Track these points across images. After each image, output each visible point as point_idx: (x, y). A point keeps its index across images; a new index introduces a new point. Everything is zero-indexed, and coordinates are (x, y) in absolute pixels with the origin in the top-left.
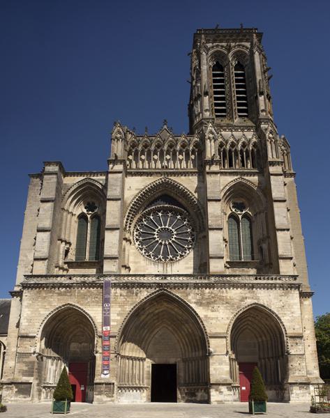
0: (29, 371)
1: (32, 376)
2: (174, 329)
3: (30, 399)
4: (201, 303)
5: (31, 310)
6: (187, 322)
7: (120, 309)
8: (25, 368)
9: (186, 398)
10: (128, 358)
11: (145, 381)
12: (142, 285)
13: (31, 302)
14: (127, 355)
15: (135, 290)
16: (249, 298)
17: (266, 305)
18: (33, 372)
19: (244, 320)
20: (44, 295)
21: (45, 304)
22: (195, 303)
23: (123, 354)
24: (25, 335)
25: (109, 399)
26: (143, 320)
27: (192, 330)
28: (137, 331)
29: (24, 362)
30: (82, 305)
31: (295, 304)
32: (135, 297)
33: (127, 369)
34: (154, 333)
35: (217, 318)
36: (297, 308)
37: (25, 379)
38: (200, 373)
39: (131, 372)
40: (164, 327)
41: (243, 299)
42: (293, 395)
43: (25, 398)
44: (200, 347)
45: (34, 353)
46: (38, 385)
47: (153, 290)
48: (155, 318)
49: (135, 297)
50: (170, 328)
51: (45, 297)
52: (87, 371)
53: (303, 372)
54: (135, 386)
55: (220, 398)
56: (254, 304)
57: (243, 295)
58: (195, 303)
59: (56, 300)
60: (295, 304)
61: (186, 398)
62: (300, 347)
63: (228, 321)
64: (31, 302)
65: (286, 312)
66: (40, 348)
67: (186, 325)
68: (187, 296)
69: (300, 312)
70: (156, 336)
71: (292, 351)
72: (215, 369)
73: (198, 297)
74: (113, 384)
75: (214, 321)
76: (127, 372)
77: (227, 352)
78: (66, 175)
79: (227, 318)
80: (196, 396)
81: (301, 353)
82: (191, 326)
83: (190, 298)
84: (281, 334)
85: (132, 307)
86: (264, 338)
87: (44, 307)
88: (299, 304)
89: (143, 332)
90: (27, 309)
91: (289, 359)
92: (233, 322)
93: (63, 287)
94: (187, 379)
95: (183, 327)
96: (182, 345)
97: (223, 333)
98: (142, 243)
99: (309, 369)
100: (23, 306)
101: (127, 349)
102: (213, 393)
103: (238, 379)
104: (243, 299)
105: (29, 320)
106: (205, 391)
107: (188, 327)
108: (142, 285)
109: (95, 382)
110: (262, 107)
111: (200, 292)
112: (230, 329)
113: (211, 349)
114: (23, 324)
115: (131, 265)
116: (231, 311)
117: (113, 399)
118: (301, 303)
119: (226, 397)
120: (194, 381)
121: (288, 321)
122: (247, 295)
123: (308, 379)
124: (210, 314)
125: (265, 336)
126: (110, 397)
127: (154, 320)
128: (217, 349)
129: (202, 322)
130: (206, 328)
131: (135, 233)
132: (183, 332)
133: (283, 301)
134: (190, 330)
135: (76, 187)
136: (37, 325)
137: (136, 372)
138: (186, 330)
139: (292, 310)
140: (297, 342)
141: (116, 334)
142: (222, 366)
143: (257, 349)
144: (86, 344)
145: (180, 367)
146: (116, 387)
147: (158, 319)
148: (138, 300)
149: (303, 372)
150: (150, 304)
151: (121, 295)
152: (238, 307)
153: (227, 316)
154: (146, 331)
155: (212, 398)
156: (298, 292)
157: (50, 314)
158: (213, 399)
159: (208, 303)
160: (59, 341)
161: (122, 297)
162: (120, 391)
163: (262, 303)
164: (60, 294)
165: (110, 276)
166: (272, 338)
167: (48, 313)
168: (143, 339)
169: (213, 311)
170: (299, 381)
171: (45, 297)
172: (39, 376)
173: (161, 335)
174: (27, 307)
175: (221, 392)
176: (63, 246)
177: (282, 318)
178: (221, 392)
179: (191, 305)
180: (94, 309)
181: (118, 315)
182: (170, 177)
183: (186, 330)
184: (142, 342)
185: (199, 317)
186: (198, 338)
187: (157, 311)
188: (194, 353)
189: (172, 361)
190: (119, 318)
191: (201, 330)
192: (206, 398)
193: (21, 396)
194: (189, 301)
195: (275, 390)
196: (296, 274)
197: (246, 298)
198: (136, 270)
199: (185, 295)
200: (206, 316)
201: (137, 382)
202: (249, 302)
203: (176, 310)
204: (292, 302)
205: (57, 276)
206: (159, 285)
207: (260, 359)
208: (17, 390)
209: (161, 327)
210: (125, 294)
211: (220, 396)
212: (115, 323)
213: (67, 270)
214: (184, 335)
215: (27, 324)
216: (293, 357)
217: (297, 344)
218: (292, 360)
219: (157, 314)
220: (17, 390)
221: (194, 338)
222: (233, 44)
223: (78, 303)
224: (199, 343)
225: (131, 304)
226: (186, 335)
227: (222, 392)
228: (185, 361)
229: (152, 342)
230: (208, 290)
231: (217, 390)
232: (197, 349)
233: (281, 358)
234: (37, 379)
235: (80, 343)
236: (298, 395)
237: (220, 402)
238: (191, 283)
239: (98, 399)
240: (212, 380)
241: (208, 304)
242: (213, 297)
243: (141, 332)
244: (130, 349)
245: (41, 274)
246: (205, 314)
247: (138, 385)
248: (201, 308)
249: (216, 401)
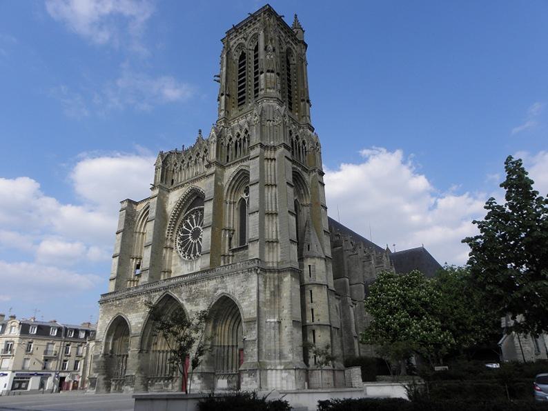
3: (95, 391)
8: (96, 367)
31: (253, 288)
47: (161, 293)
60: (253, 288)
62: (254, 332)
78: (137, 204)
98: (182, 246)
110: (262, 87)
115: (173, 269)
122: (219, 286)
131: (178, 238)
135: (142, 211)
139: (251, 294)
164: (116, 306)
169: (196, 306)
176: (134, 263)
182: (195, 184)
198: (175, 272)
202: (219, 292)
213: (138, 281)
222: (248, 31)
230: (193, 287)
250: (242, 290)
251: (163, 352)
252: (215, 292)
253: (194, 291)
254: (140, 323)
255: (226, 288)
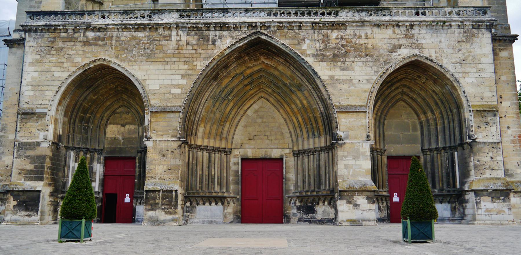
0: (37, 172)
1: (41, 179)
2: (278, 101)
3: (37, 218)
4: (324, 56)
5: (40, 69)
6: (299, 87)
7: (186, 67)
9: (299, 215)
10: (202, 149)
11: (232, 187)
12: (223, 26)
13: (38, 57)
14: (199, 143)
15: (211, 34)
16: (405, 46)
17: (434, 58)
18: (42, 173)
19: (398, 85)
20: (61, 44)
21: (63, 60)
22: (313, 55)
23: (193, 142)
24: (29, 111)
25: (169, 217)
26: (226, 87)
27: (309, 102)
28: (217, 105)
29: (28, 157)
30: (122, 60)
32: (210, 46)
33: (199, 167)
34: (245, 108)
35: (351, 80)
36: (488, 62)
37: (29, 185)
38: (323, 173)
39: (206, 173)
40: (263, 91)
41: (394, 48)
42: (480, 212)
43: (29, 216)
44: (321, 129)
45: (46, 140)
46: (52, 194)
48: (246, 82)
49: (210, 46)
50: (271, 99)
51: (61, 49)
52: (135, 171)
53: (499, 172)
54: (214, 194)
55: (355, 215)
56: (414, 56)
57: (395, 42)
58: (313, 55)
59: (81, 52)
60: (485, 56)
61: (299, 215)
62: (493, 129)
63: (368, 87)
64: (38, 57)
65: (468, 70)
66: (55, 133)
67: (299, 94)
68: (299, 43)
69: (493, 70)
70: (249, 112)
71: (480, 137)
72: (346, 166)
73: (319, 46)
74: (176, 191)
75: (344, 86)
76: (199, 172)
77: (368, 136)
79: (368, 81)
80: (314, 212)
81: (496, 139)
82: (307, 95)
83: (304, 47)
84: (459, 107)
85: (207, 63)
86: (429, 114)
87: (60, 65)
88: (491, 56)
89: (227, 105)
90: (32, 69)
91: (475, 149)
92: (377, 87)
93: (94, 30)
94: (300, 183)
95: (295, 98)
96: (291, 127)
97: (361, 106)
99: (508, 167)
100: (26, 64)
101: (200, 133)
102: (342, 205)
103: (386, 184)
104: (394, 48)
105: (36, 87)
106: (329, 204)
107: (302, 98)
108: (223, 26)
109: (145, 188)
111: (321, 37)
112: (373, 98)
113: (340, 133)
114: (26, 93)
116: (375, 68)
117: (176, 216)
118: (495, 54)
119: (365, 212)
120: (312, 188)
121: (473, 85)
122: (403, 42)
123: (508, 183)
124: (338, 74)
125: (432, 111)
126: (171, 213)
127: (246, 86)
128: (351, 133)
129: (324, 86)
130: (332, 97)
132: (293, 106)
133: (464, 50)
134: (305, 102)
136: (49, 94)
137: (216, 172)
138: (298, 102)
139: (480, 66)
140: (489, 119)
141: (181, 109)
142: (358, 162)
143: (419, 133)
144: (132, 127)
145: (290, 162)
146: (180, 198)
147: (251, 83)
148: (216, 52)
149: (499, 172)
150: (237, 58)
151: (188, 44)
152: (386, 63)
153: (367, 78)
154: (231, 104)
155: (340, 214)
156: (489, 36)
157: (70, 75)
158: (342, 217)
159: (335, 55)
160: (88, 122)
161: (190, 47)
162: (188, 204)
163: (427, 55)
164: (86, 43)
165: (170, 11)
166: (445, 114)
167: (66, 74)
168: (227, 117)
169: (343, 69)
170: (492, 187)
171: (61, 49)
172: (53, 180)
173: (256, 111)
174: (32, 64)
175: (356, 206)
177: (461, 81)
178: (356, 206)
179: (308, 59)
180: (145, 67)
181: (183, 76)
183: (298, 102)
184: (225, 121)
185: (319, 78)
186: (318, 115)
187: (248, 72)
188: (311, 141)
189: (275, 153)
190: (184, 82)
191: (323, 100)
192: (332, 216)
193: (23, 213)
194: (304, 52)
195: (449, 202)
196: (486, 5)
197: (400, 46)
199: (296, 42)
200: (332, 78)
201: (217, 188)
203: (280, 68)
204: (478, 52)
205: (82, 14)
206: (251, 26)
207: (423, 151)
208: (15, 203)
209: (256, 98)
210: (194, 42)
211: (356, 211)
212: (178, 91)
214: (296, 110)
215: (32, 93)
216: (479, 146)
217: (487, 124)
218: (479, 151)
219: (251, 75)
220: (15, 203)
221: (311, 115)
223: (117, 57)
224: (320, 124)
225: (205, 59)
226: (299, 110)
227: (359, 205)
228: (296, 154)
229: (242, 123)
230: (334, 34)
231: (349, 202)
232: (316, 133)
233: (459, 148)
234: (50, 185)
235: (123, 125)
236: (487, 210)
237: (354, 222)
238: (306, 22)
239: (151, 218)
240: (342, 186)
241: (336, 57)
242: (343, 46)
243: (223, 107)
244: (204, 133)
245: (56, 10)
246: (331, 73)
247: (220, 195)
248: (324, 64)
249: (347, 221)
250: (460, 55)
251: (206, 149)
252: (392, 51)
253: (334, 42)
254: (176, 86)
255: (420, 47)
